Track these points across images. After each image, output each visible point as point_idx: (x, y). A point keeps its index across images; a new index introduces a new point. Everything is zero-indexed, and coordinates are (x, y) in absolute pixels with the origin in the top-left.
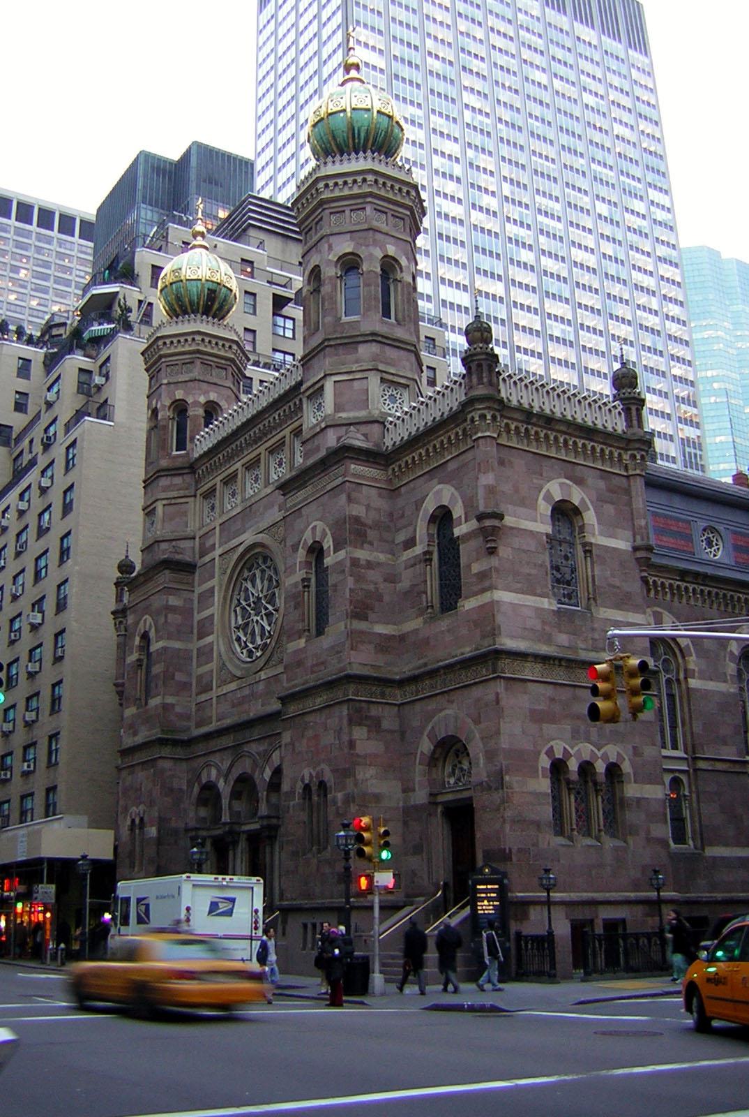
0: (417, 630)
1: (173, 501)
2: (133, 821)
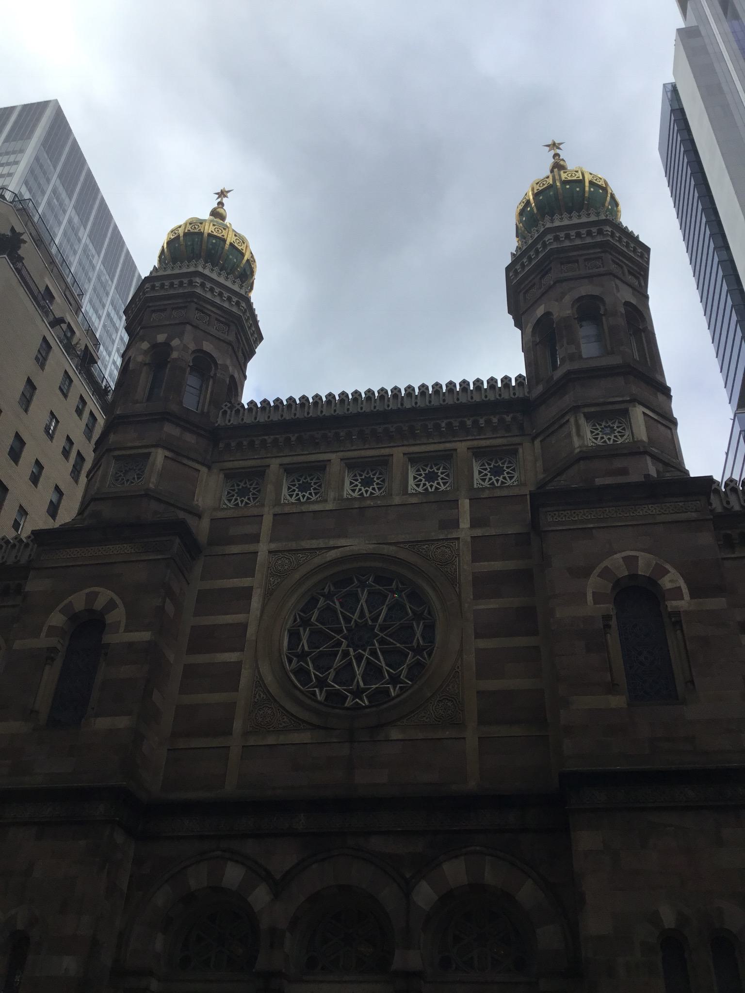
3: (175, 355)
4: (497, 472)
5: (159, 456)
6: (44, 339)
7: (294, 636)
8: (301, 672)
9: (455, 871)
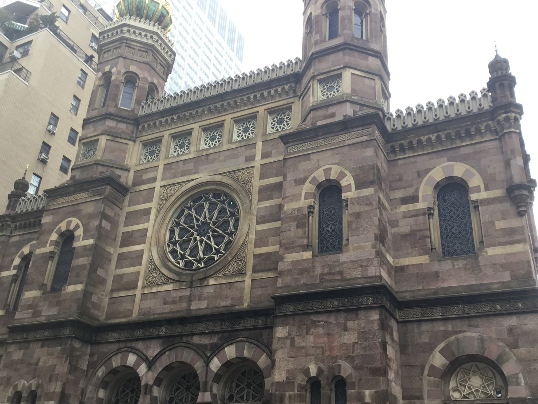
0: (422, 264)
3: (113, 78)
4: (280, 122)
5: (103, 140)
6: (82, 70)
7: (172, 232)
8: (174, 252)
9: (230, 352)
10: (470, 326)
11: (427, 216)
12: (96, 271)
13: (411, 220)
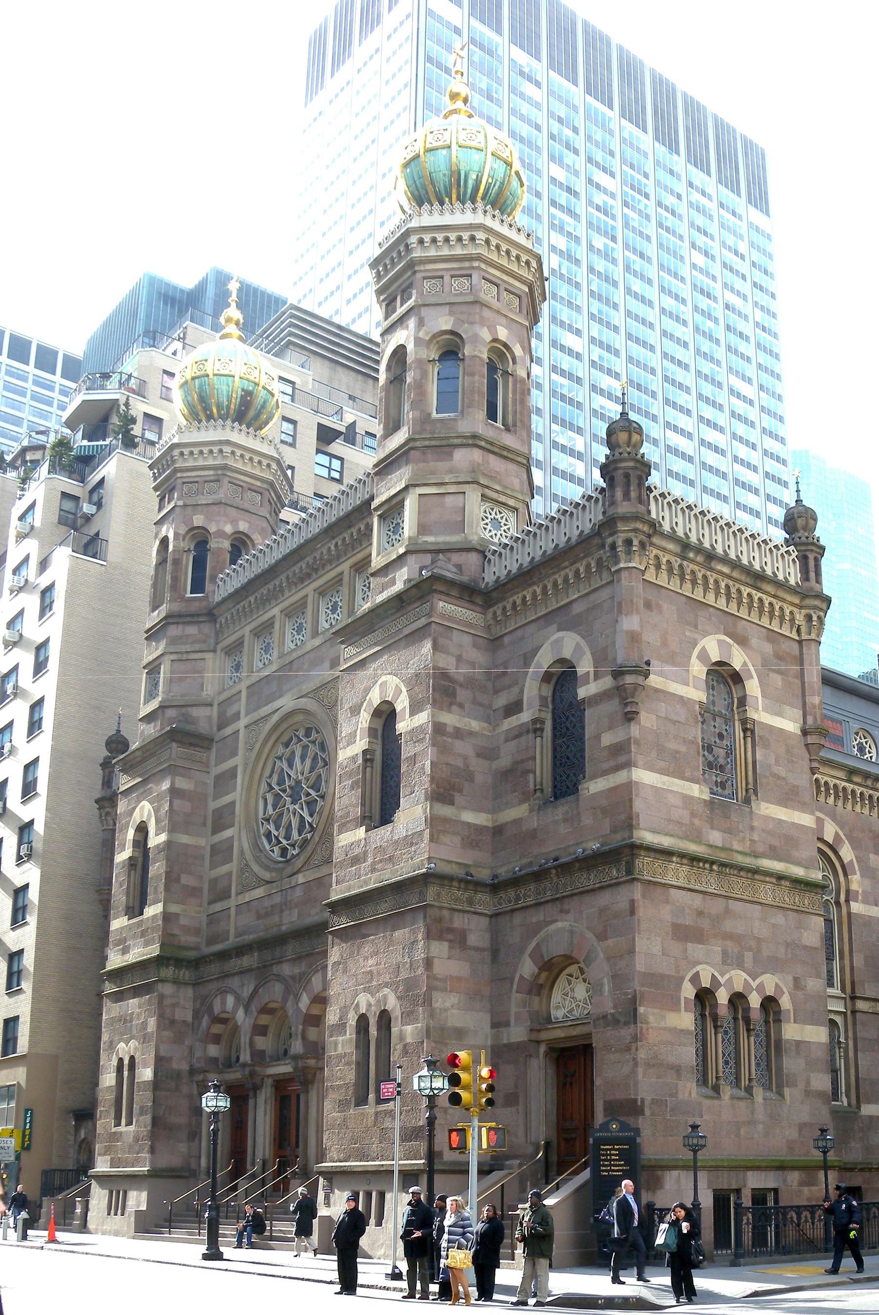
0: (521, 819)
1: (185, 657)
2: (121, 1060)
10: (562, 911)
11: (531, 735)
12: (178, 880)
13: (513, 744)
